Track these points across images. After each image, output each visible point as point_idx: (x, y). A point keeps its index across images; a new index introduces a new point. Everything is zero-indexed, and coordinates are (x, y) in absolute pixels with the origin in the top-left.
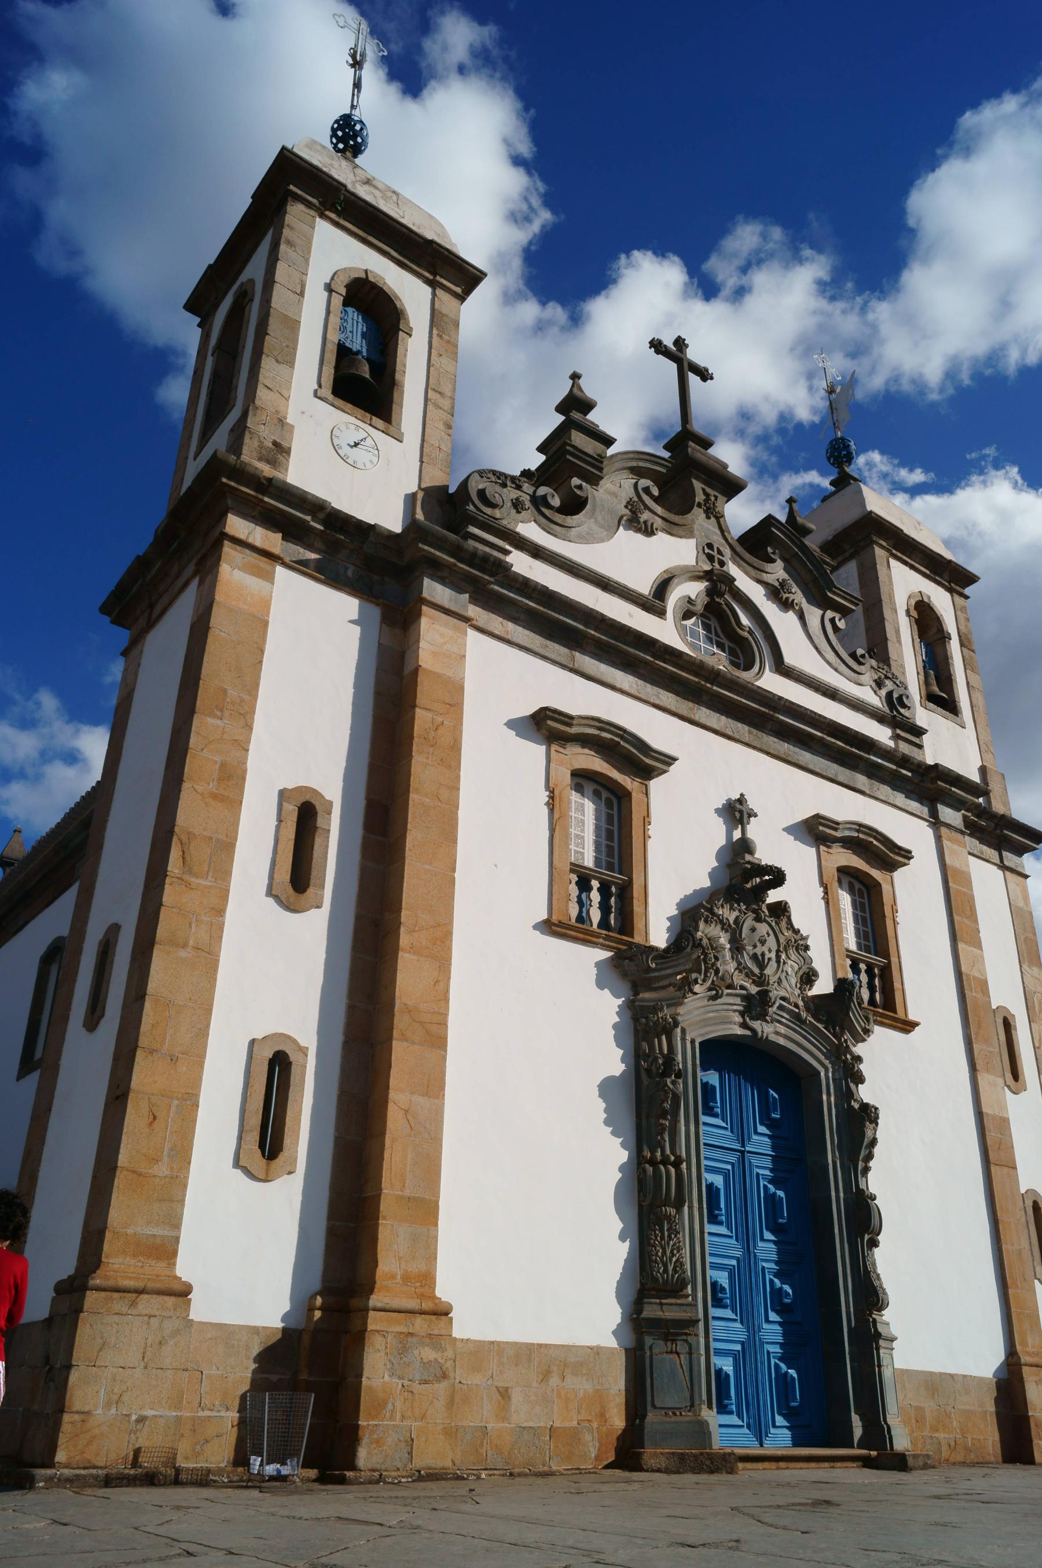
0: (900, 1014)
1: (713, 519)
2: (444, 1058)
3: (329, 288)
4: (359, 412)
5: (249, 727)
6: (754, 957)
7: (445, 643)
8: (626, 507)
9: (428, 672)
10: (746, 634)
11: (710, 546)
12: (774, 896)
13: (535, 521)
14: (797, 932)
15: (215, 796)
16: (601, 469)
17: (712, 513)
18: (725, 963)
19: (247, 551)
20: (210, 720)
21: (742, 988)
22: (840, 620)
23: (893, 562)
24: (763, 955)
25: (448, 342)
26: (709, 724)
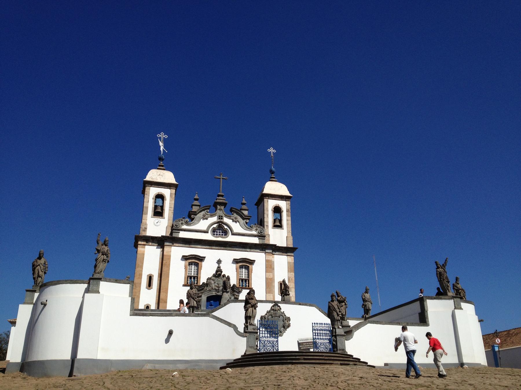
0: (250, 287)
2: (167, 304)
4: (158, 217)
5: (142, 268)
9: (165, 255)
10: (226, 230)
11: (220, 216)
12: (223, 274)
15: (139, 278)
18: (212, 285)
19: (141, 245)
20: (138, 269)
21: (215, 288)
23: (269, 200)
24: (219, 283)
26: (215, 248)
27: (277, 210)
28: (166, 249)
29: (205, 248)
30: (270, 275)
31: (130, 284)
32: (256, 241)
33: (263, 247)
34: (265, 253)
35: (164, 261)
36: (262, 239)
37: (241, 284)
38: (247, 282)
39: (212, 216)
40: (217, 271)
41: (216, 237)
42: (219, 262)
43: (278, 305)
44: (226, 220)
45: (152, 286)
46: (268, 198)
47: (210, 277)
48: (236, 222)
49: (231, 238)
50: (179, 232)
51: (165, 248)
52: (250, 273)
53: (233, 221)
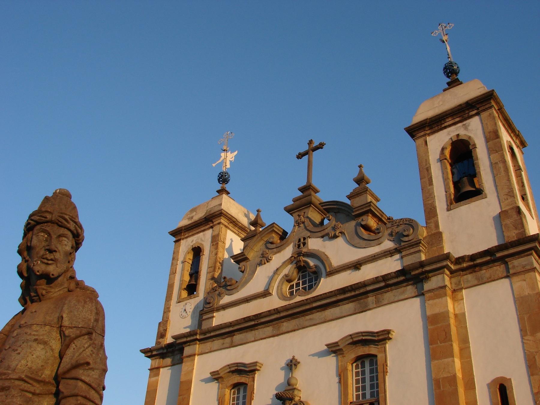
1: (302, 225)
7: (188, 368)
8: (261, 257)
10: (314, 269)
11: (299, 240)
13: (226, 295)
16: (245, 255)
17: (300, 224)
23: (428, 139)
25: (216, 244)
29: (264, 336)
34: (421, 294)
48: (335, 237)
50: (213, 317)
52: (380, 375)
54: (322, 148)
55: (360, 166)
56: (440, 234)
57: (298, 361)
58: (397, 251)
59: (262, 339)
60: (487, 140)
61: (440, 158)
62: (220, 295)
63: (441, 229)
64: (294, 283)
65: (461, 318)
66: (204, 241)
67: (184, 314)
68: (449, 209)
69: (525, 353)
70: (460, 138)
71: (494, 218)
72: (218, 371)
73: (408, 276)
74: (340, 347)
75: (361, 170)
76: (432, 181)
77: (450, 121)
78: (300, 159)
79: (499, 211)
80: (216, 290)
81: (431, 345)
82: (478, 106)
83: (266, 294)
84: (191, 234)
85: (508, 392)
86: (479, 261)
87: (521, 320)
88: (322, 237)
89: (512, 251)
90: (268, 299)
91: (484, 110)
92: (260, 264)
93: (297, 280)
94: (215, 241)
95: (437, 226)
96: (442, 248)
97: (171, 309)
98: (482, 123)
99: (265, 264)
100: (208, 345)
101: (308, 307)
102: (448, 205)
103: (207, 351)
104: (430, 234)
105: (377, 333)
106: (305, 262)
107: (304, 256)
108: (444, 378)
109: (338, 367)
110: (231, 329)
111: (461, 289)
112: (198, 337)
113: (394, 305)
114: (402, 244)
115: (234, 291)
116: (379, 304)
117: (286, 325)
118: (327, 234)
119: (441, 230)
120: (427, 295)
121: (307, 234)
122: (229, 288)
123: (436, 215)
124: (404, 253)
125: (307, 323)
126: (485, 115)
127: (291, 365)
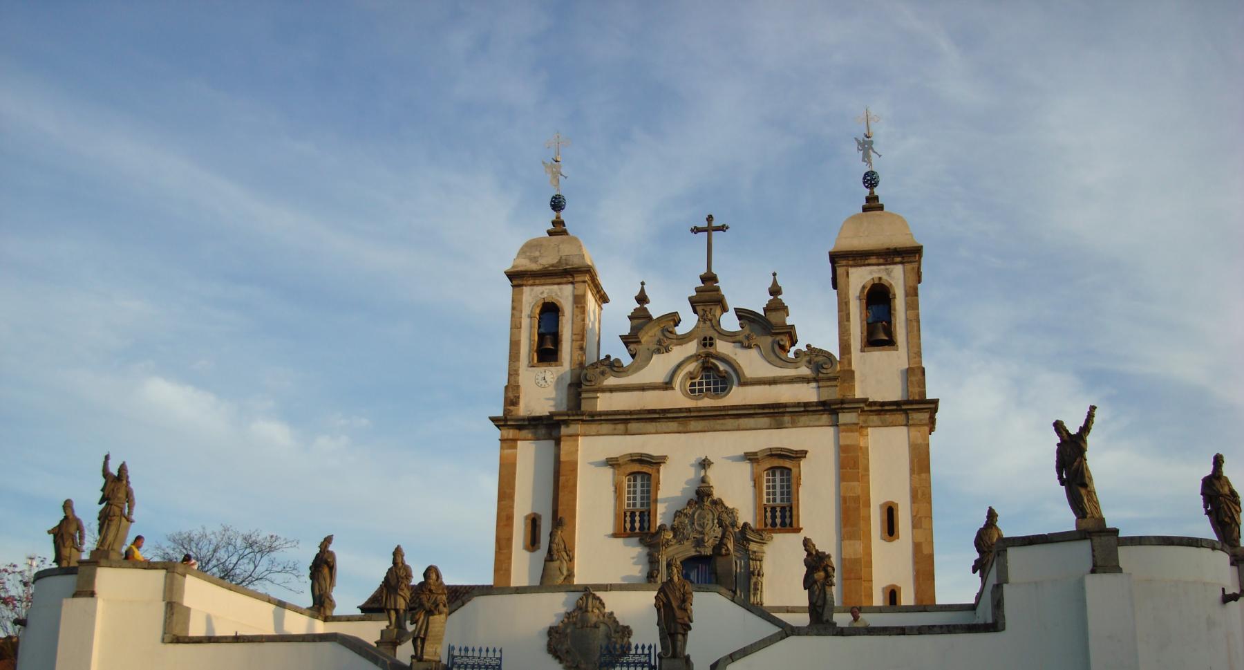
0: (795, 525)
1: (708, 323)
3: (531, 317)
4: (545, 364)
6: (700, 525)
9: (563, 462)
10: (724, 374)
11: (705, 339)
14: (727, 508)
15: (506, 525)
20: (503, 502)
21: (694, 538)
22: (782, 340)
23: (851, 270)
24: (704, 523)
26: (695, 430)
27: (878, 297)
28: (565, 446)
30: (857, 487)
31: (166, 569)
32: (808, 393)
33: (829, 409)
34: (836, 425)
35: (561, 478)
36: (828, 386)
37: (769, 521)
38: (788, 514)
39: (684, 339)
40: (698, 492)
41: (697, 398)
42: (705, 464)
43: (594, 595)
44: (722, 347)
45: (539, 542)
46: (844, 262)
47: (679, 509)
48: (749, 347)
49: (738, 396)
50: (598, 397)
51: (562, 443)
52: (794, 487)
53: (743, 347)
54: (725, 231)
55: (774, 274)
56: (852, 372)
57: (712, 461)
58: (816, 380)
59: (665, 433)
60: (907, 295)
61: (860, 296)
62: (603, 373)
63: (854, 367)
64: (697, 380)
65: (865, 451)
66: (561, 298)
67: (543, 382)
68: (862, 351)
69: (911, 486)
70: (882, 282)
71: (902, 371)
72: (617, 458)
73: (827, 408)
74: (758, 457)
75: (775, 280)
76: (849, 318)
77: (873, 260)
78: (695, 233)
79: (907, 367)
80: (597, 367)
81: (842, 469)
82: (904, 255)
83: (667, 385)
84: (537, 282)
85: (895, 512)
86: (887, 408)
87: (912, 462)
88: (734, 342)
89: (915, 406)
90: (669, 392)
91: (908, 262)
92: (659, 351)
93: (699, 378)
94: (579, 301)
95: (850, 363)
96: (852, 388)
97: (520, 372)
98: (905, 275)
99: (663, 353)
100: (594, 428)
101: (723, 413)
102: (862, 347)
103: (592, 434)
104: (842, 369)
105: (796, 451)
106: (714, 364)
107: (712, 357)
108: (850, 496)
109: (753, 473)
110: (629, 417)
111: (868, 427)
112: (584, 418)
113: (809, 429)
114: (820, 375)
115: (624, 374)
116: (794, 425)
117: (693, 424)
118: (740, 342)
119: (853, 368)
120: (842, 428)
121: (715, 335)
122: (615, 369)
123: (850, 353)
124: (821, 384)
125: (718, 427)
126: (909, 266)
127: (704, 464)
